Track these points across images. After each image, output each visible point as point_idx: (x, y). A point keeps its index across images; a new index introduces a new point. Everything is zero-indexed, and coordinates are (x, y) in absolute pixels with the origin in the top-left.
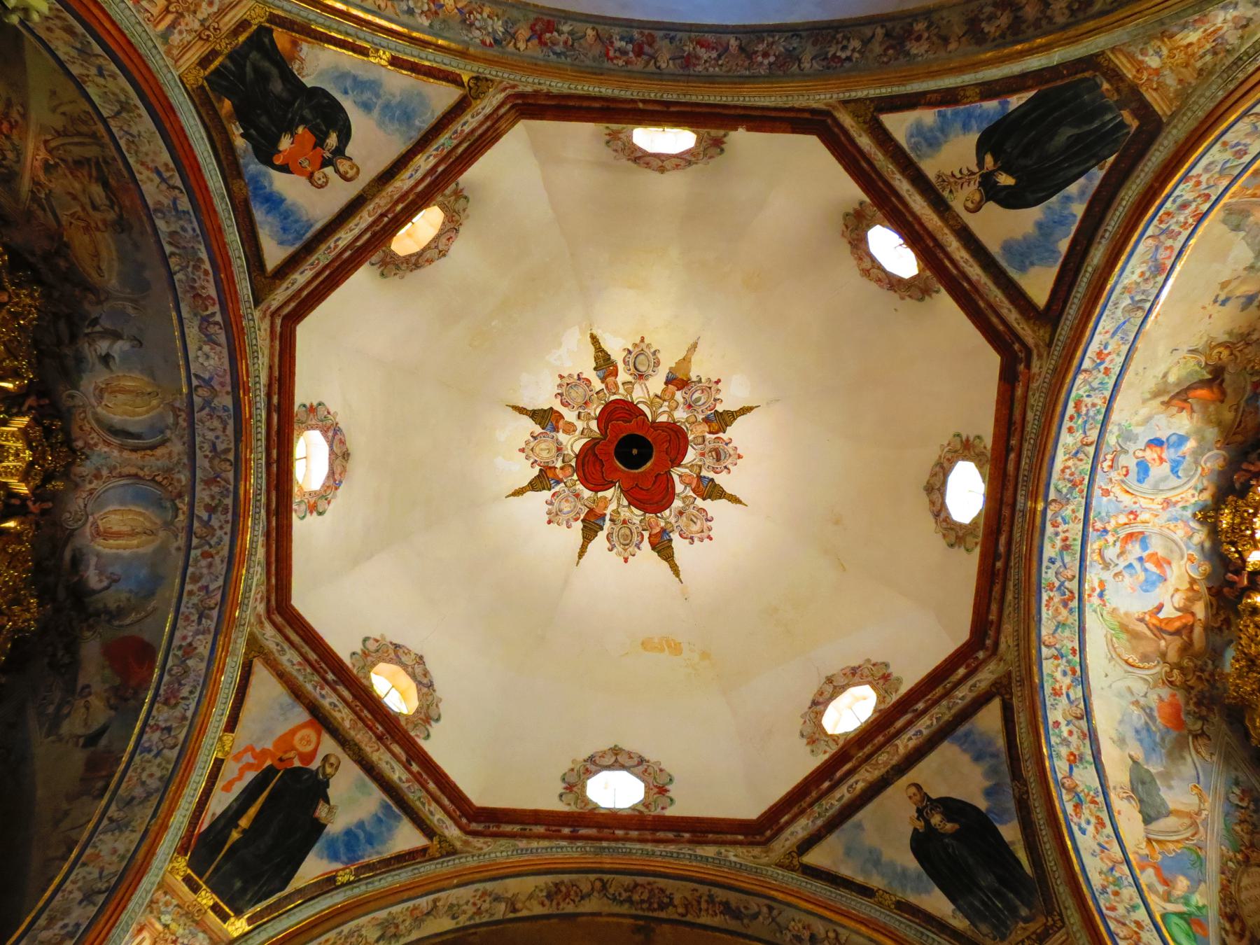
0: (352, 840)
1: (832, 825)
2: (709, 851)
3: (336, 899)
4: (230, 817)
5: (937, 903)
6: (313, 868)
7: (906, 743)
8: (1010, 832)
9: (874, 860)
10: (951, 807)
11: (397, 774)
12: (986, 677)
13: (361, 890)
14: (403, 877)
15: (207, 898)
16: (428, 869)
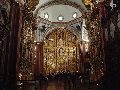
0: (47, 27)
1: (72, 24)
2: (66, 24)
3: (47, 30)
4: (42, 29)
5: (77, 29)
6: (46, 29)
7: (77, 22)
8: (80, 27)
9: (74, 26)
10: (78, 25)
11: (48, 23)
12: (81, 20)
13: (48, 29)
14: (50, 28)
15: (42, 32)
16: (51, 27)
